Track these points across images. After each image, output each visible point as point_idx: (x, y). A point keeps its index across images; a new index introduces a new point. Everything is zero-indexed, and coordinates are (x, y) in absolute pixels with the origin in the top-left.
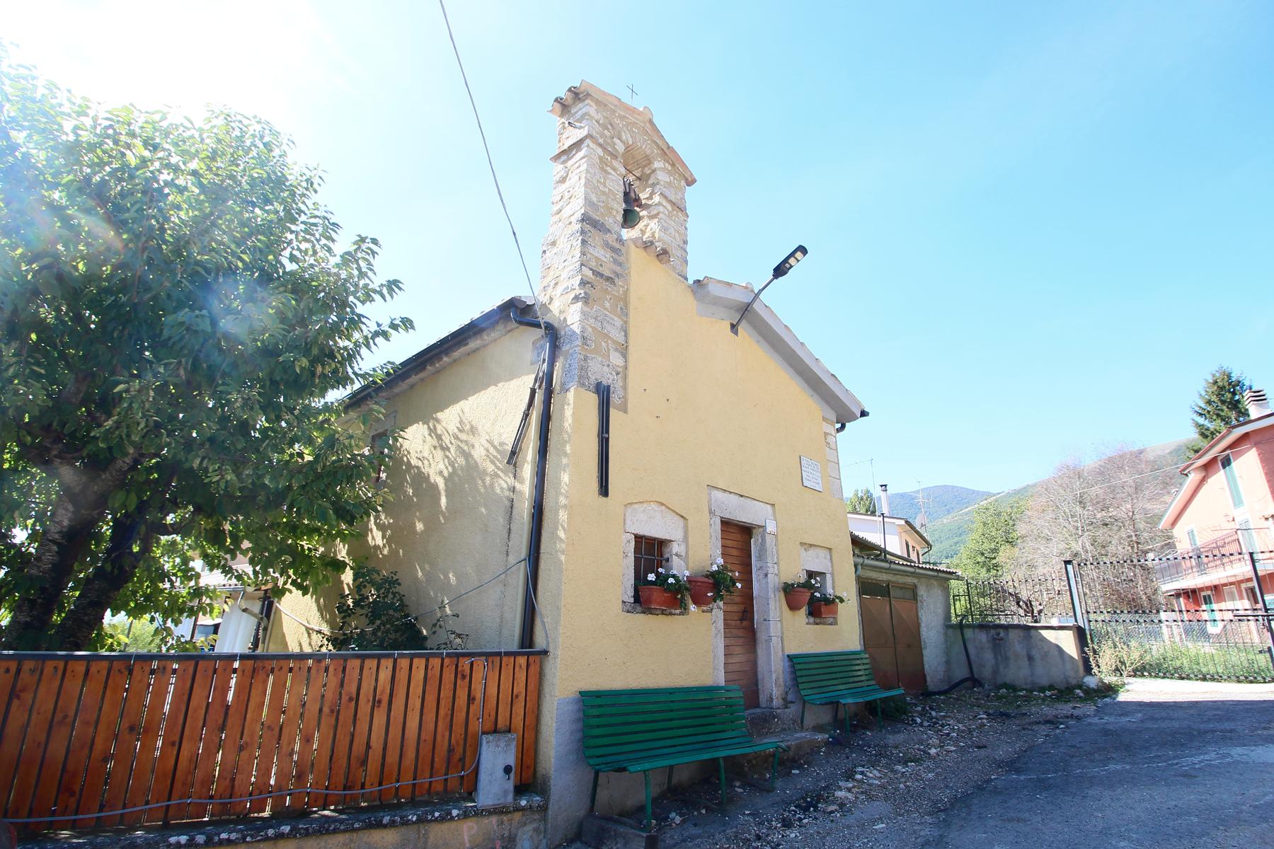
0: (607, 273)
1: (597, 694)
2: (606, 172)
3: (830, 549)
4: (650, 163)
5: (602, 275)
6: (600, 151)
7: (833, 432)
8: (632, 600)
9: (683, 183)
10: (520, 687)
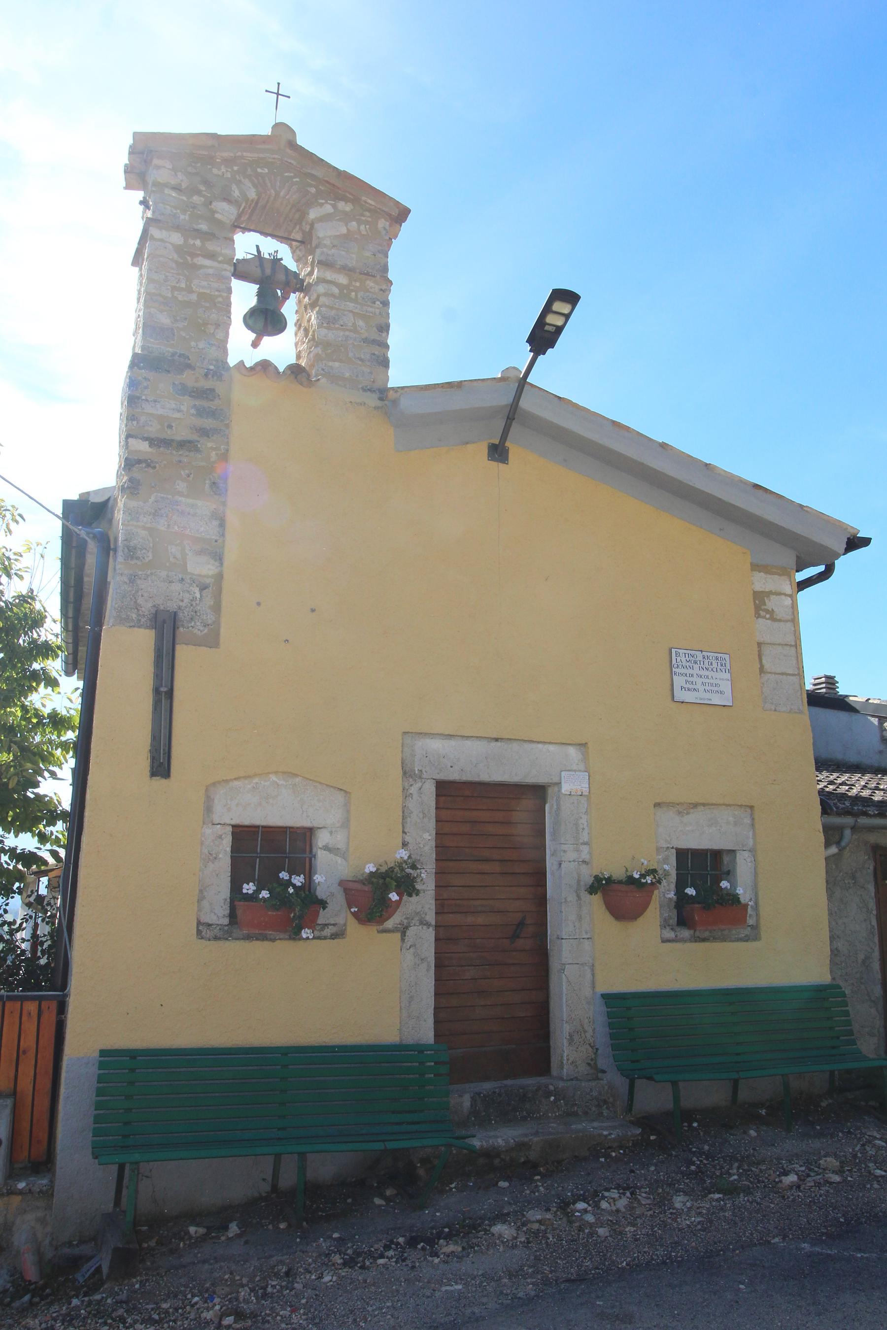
0: (181, 433)
1: (133, 1054)
2: (195, 267)
3: (752, 807)
4: (304, 215)
6: (176, 238)
7: (788, 589)
8: (226, 921)
9: (382, 223)
10: (29, 1042)
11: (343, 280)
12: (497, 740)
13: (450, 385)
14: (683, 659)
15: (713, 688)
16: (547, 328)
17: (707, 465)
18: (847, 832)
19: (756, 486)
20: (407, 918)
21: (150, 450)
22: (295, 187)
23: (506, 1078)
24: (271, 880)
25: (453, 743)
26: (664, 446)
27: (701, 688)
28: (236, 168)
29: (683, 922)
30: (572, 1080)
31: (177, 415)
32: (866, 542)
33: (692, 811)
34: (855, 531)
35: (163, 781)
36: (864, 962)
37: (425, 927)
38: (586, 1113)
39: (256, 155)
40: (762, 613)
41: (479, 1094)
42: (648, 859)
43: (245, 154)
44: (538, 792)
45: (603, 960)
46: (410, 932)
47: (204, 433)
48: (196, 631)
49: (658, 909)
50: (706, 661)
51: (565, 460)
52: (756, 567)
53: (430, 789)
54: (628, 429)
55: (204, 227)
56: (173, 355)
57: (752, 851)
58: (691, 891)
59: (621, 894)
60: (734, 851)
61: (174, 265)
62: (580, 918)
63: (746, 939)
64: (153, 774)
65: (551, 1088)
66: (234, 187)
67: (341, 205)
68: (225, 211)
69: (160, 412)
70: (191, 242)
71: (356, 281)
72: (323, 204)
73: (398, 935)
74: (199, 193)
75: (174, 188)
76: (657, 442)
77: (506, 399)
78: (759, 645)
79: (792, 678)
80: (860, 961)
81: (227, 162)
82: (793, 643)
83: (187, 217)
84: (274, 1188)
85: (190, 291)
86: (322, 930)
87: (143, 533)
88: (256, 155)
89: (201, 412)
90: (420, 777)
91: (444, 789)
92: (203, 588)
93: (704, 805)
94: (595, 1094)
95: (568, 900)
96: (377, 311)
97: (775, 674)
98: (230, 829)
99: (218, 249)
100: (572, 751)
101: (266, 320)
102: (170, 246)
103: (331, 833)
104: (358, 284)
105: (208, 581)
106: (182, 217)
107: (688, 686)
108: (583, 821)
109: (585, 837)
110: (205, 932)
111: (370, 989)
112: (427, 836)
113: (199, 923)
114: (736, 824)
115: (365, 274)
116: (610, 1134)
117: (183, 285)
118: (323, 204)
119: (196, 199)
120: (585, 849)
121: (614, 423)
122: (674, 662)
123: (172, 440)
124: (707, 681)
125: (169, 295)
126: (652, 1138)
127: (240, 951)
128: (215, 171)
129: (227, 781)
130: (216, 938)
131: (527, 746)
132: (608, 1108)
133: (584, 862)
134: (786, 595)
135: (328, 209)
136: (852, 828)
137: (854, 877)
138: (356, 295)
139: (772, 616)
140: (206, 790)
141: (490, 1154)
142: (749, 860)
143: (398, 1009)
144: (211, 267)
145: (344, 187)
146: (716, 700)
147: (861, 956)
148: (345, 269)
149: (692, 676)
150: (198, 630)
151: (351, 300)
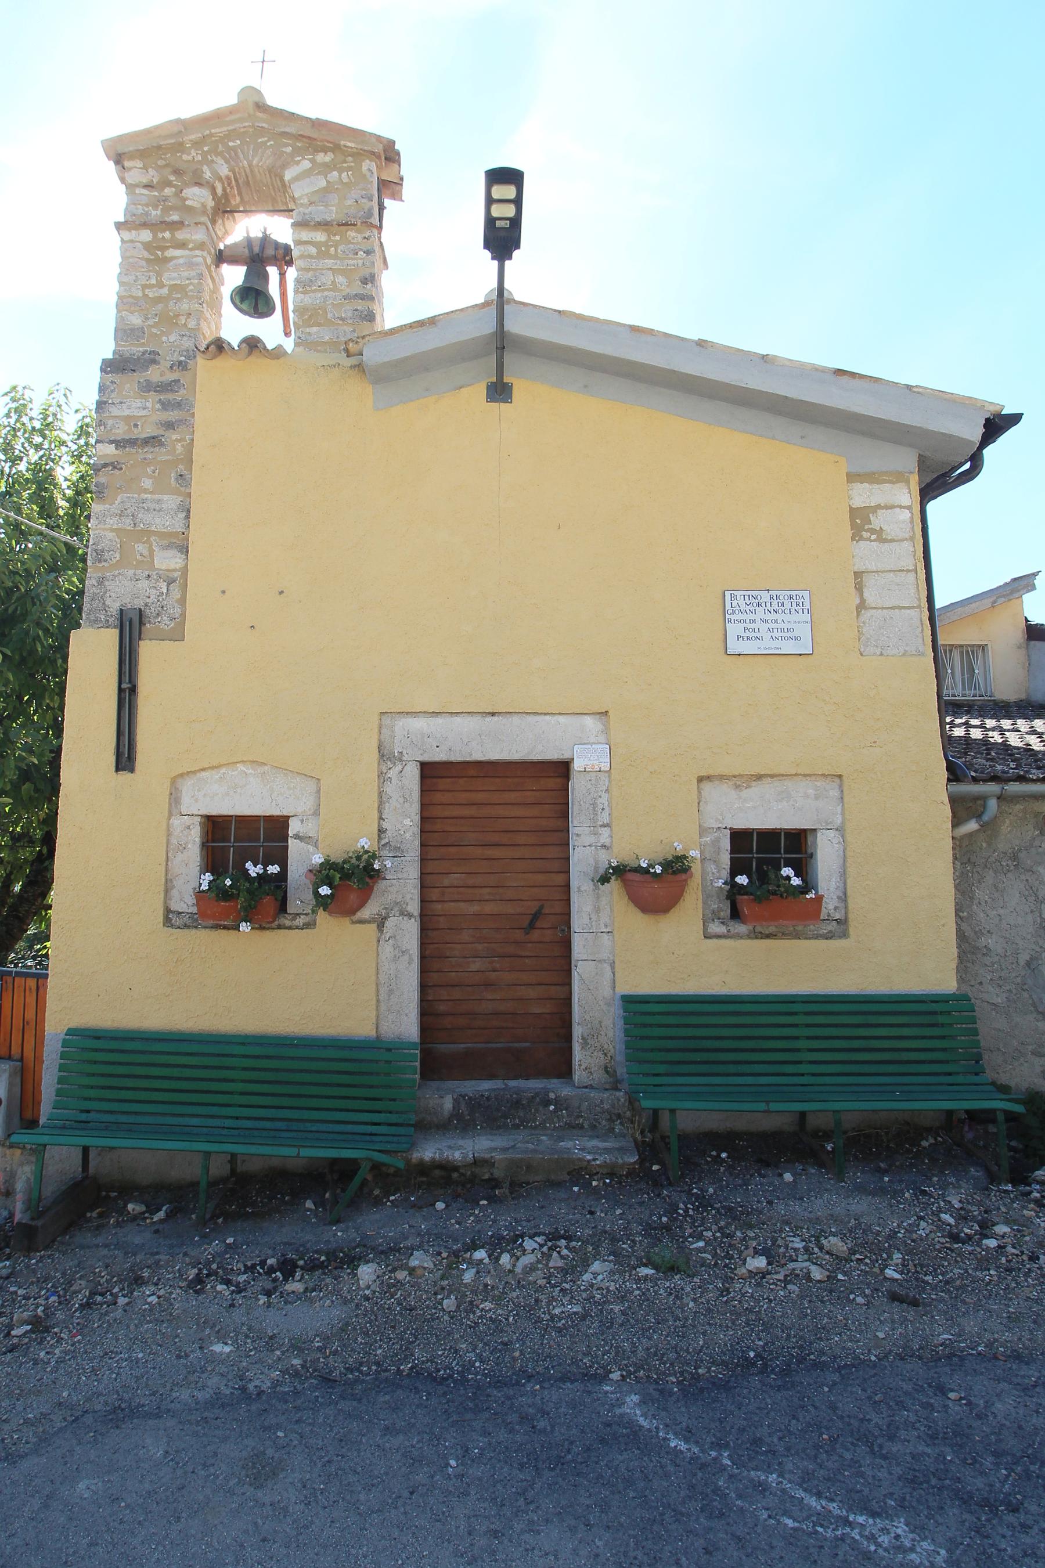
0: (148, 430)
2: (167, 260)
3: (840, 776)
5: (132, 442)
11: (320, 236)
12: (493, 714)
13: (420, 324)
14: (742, 602)
15: (783, 634)
17: (764, 358)
18: (993, 803)
19: (839, 372)
20: (386, 908)
21: (117, 452)
22: (269, 152)
23: (516, 1078)
24: (244, 871)
25: (439, 720)
26: (701, 344)
27: (767, 636)
28: (206, 149)
29: (735, 914)
30: (586, 1087)
31: (144, 413)
32: (1015, 419)
33: (754, 784)
34: (997, 408)
35: (130, 774)
36: (1028, 964)
37: (406, 918)
38: (593, 1127)
39: (225, 129)
40: (865, 534)
41: (463, 1097)
42: (685, 840)
43: (213, 131)
44: (562, 769)
45: (623, 957)
46: (390, 923)
47: (170, 426)
48: (162, 626)
49: (700, 902)
50: (775, 602)
51: (586, 386)
52: (853, 478)
53: (413, 773)
54: (650, 332)
55: (175, 217)
56: (144, 353)
57: (841, 830)
58: (742, 880)
60: (815, 830)
61: (144, 263)
62: (597, 910)
63: (829, 936)
64: (118, 769)
65: (552, 1096)
66: (205, 168)
67: (321, 157)
68: (197, 196)
69: (127, 413)
70: (160, 235)
71: (335, 235)
72: (299, 161)
73: (374, 926)
74: (169, 184)
75: (146, 186)
76: (693, 341)
77: (489, 327)
78: (858, 575)
79: (908, 611)
80: (1022, 963)
81: (197, 144)
82: (911, 567)
83: (159, 212)
84: (233, 1171)
85: (160, 285)
86: (294, 919)
87: (111, 535)
88: (225, 129)
89: (165, 406)
90: (401, 760)
91: (429, 772)
92: (170, 582)
93: (772, 776)
94: (606, 1106)
95: (582, 889)
96: (360, 262)
97: (883, 608)
98: (199, 819)
99: (188, 236)
100: (588, 721)
101: (253, 298)
102: (139, 245)
103: (302, 821)
104: (338, 238)
105: (176, 574)
106: (154, 213)
107: (748, 634)
108: (604, 800)
109: (604, 818)
110: (178, 922)
111: (347, 982)
112: (407, 822)
113: (168, 911)
114: (817, 798)
115: (343, 225)
116: (595, 1160)
117: (154, 282)
118: (299, 161)
119: (168, 191)
120: (605, 832)
121: (634, 329)
122: (728, 606)
123: (137, 439)
124: (775, 626)
125: (140, 294)
126: (655, 1168)
127: (204, 939)
128: (185, 157)
129: (194, 772)
130: (186, 926)
131: (531, 719)
132: (621, 1124)
133: (603, 846)
134: (901, 507)
135: (306, 164)
136: (998, 798)
138: (336, 250)
139: (880, 536)
140: (174, 781)
141: (446, 1168)
142: (835, 841)
143: (374, 1002)
144: (182, 257)
145: (323, 139)
146: (788, 647)
147: (1024, 957)
148: (323, 225)
149: (754, 621)
150: (165, 623)
151: (330, 257)
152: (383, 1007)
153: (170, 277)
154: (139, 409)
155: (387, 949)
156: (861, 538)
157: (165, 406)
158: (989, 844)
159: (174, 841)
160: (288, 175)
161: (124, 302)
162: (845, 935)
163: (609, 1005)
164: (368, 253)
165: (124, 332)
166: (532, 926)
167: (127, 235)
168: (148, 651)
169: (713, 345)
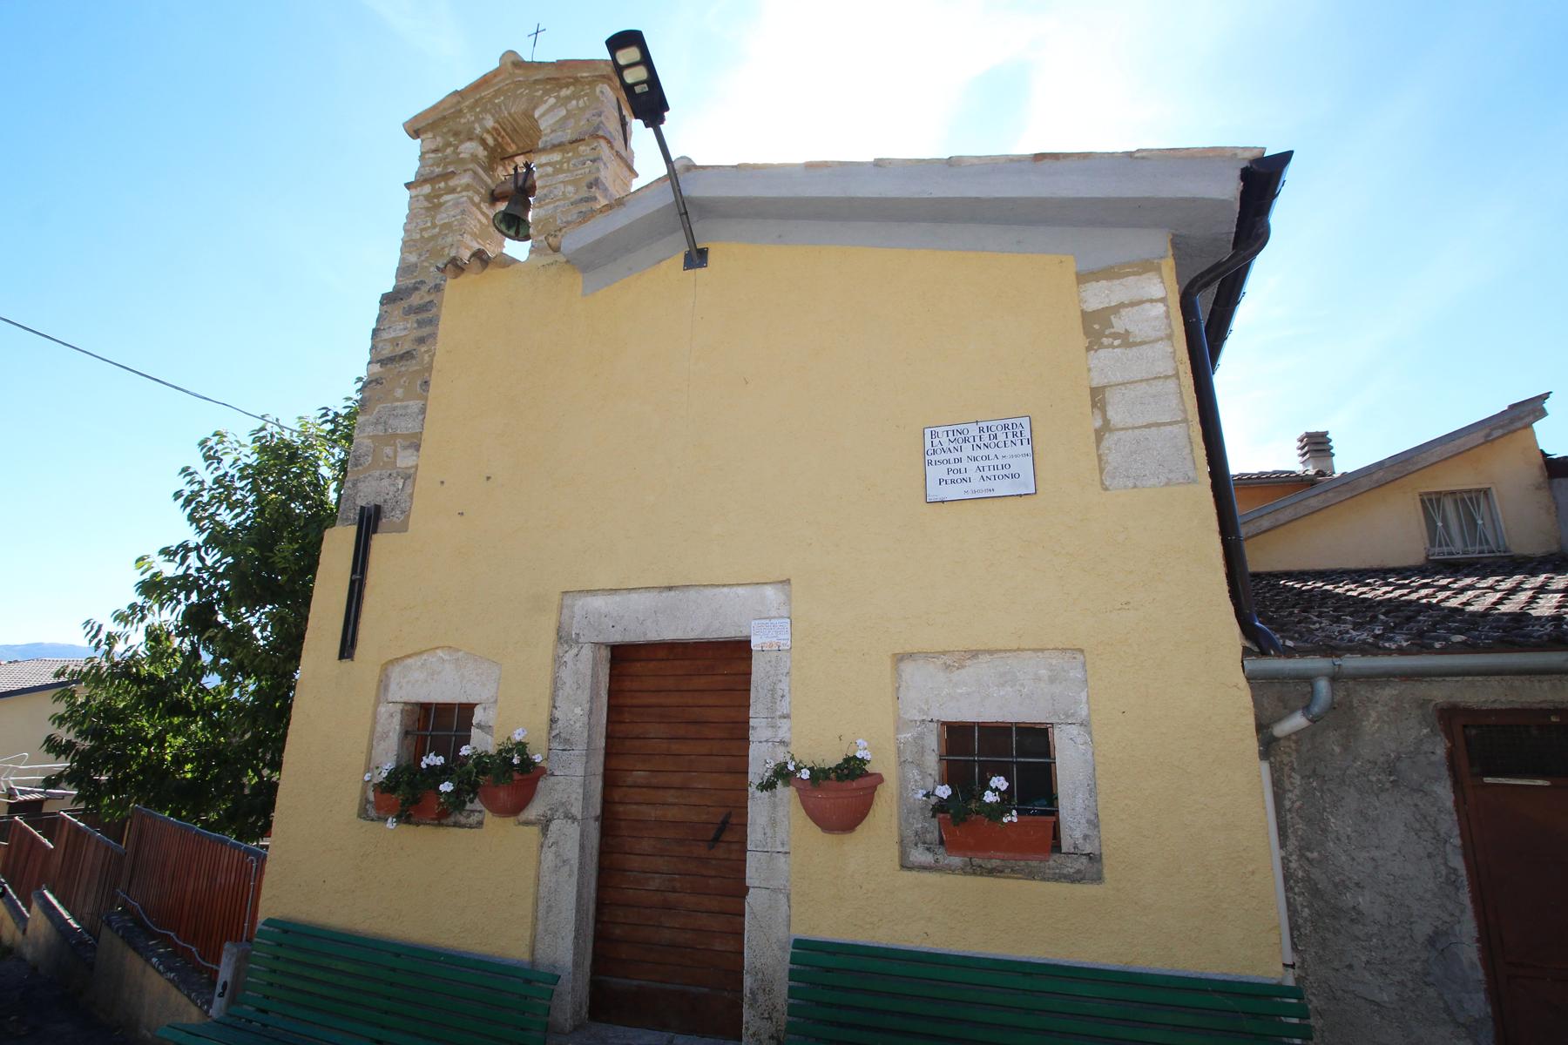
11: (556, 157)
12: (670, 588)
14: (944, 440)
15: (996, 473)
16: (638, 89)
18: (1323, 686)
19: (1039, 157)
25: (617, 598)
27: (976, 476)
33: (968, 662)
36: (1432, 941)
40: (1105, 341)
46: (554, 826)
50: (985, 436)
52: (1083, 278)
59: (840, 793)
63: (1076, 878)
67: (565, 92)
69: (393, 335)
73: (535, 830)
74: (449, 144)
79: (1169, 428)
81: (471, 108)
89: (420, 324)
93: (991, 652)
97: (1134, 428)
100: (769, 591)
107: (952, 476)
109: (783, 707)
111: (509, 893)
112: (578, 711)
119: (449, 150)
120: (785, 724)
122: (928, 445)
124: (987, 463)
129: (402, 659)
131: (709, 592)
133: (782, 742)
134: (1152, 301)
135: (552, 101)
137: (1391, 769)
139: (1126, 340)
142: (1080, 740)
146: (1003, 488)
147: (1423, 929)
149: (960, 460)
152: (541, 927)
153: (442, 218)
154: (403, 329)
155: (549, 857)
156: (1102, 346)
157: (420, 324)
158: (1345, 748)
159: (379, 729)
160: (537, 114)
161: (407, 246)
162: (1098, 878)
163: (782, 949)
164: (593, 161)
165: (404, 270)
166: (716, 839)
167: (414, 192)
168: (378, 542)
169: (890, 162)
